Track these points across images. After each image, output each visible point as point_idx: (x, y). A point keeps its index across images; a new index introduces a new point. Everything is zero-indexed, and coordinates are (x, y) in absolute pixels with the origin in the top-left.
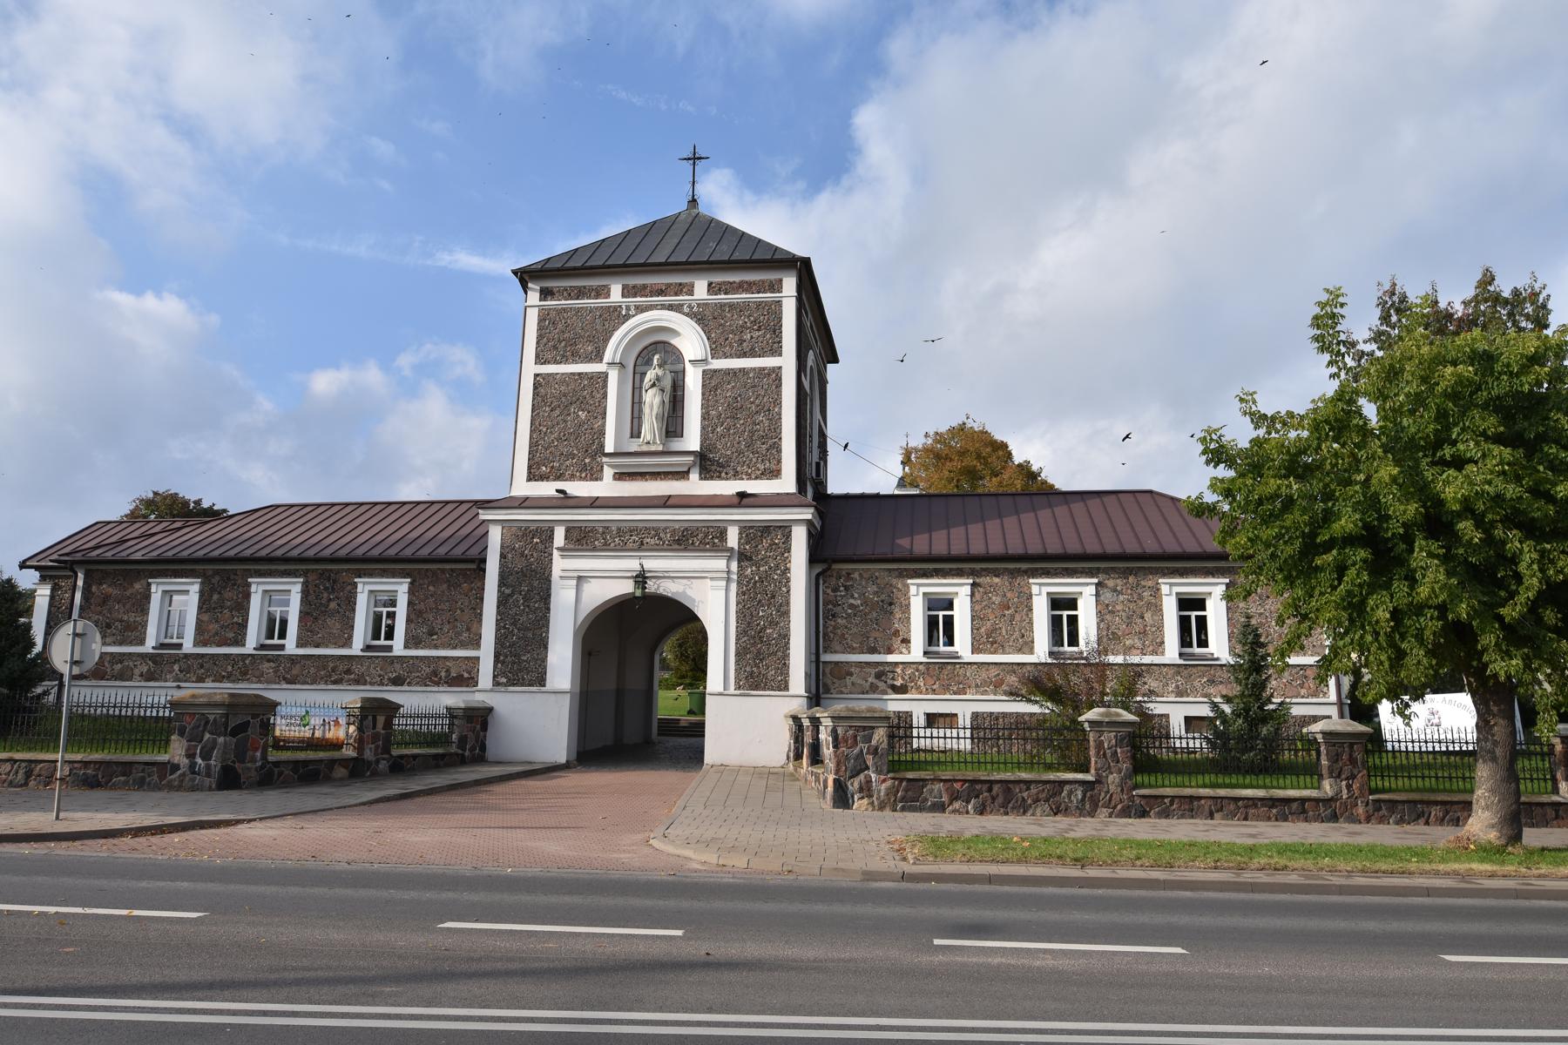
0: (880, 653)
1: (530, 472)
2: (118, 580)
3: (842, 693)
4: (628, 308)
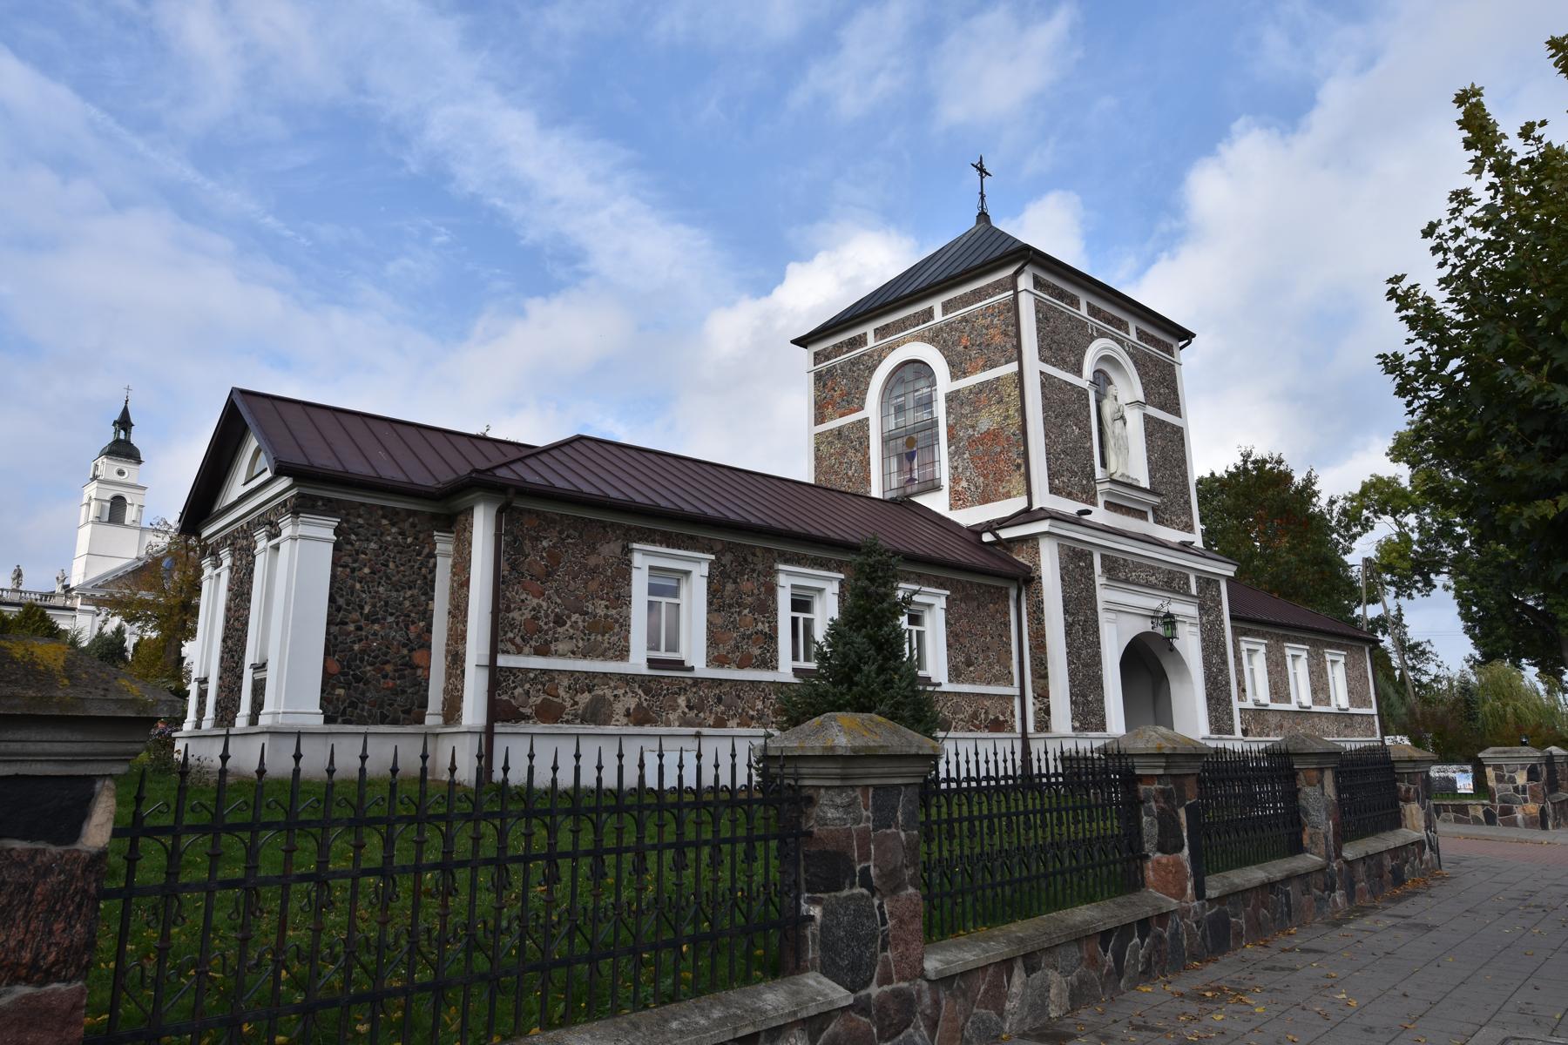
2: (568, 536)
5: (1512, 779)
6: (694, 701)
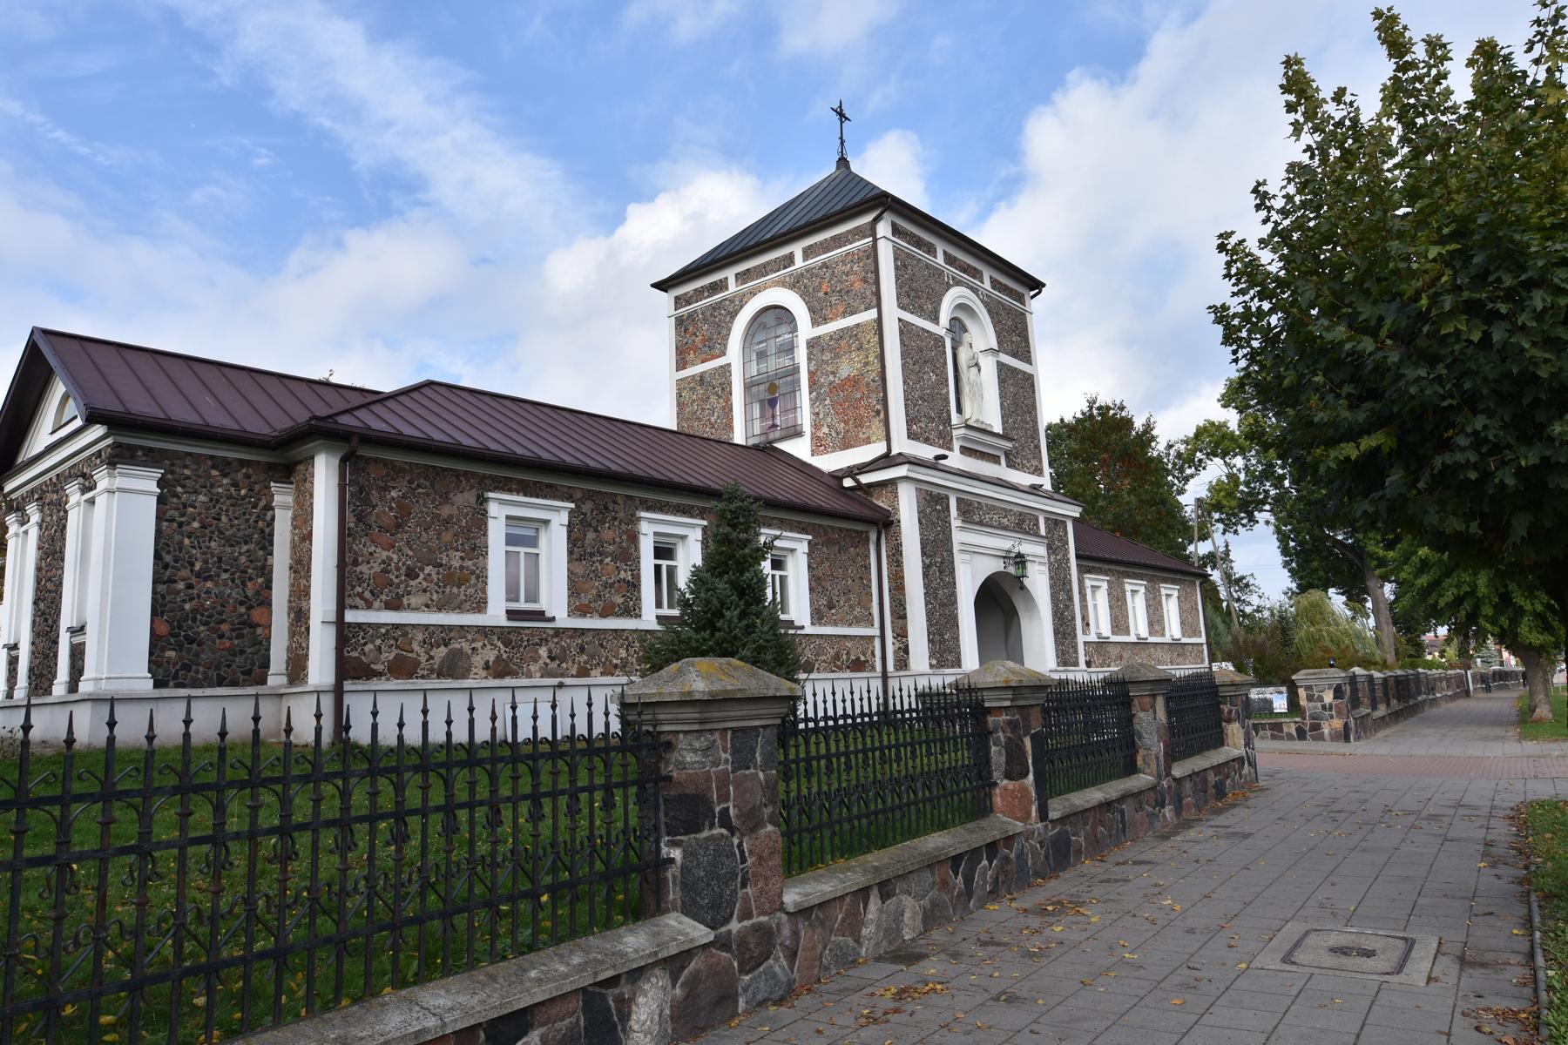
2: (419, 486)
5: (1321, 699)
6: (556, 651)
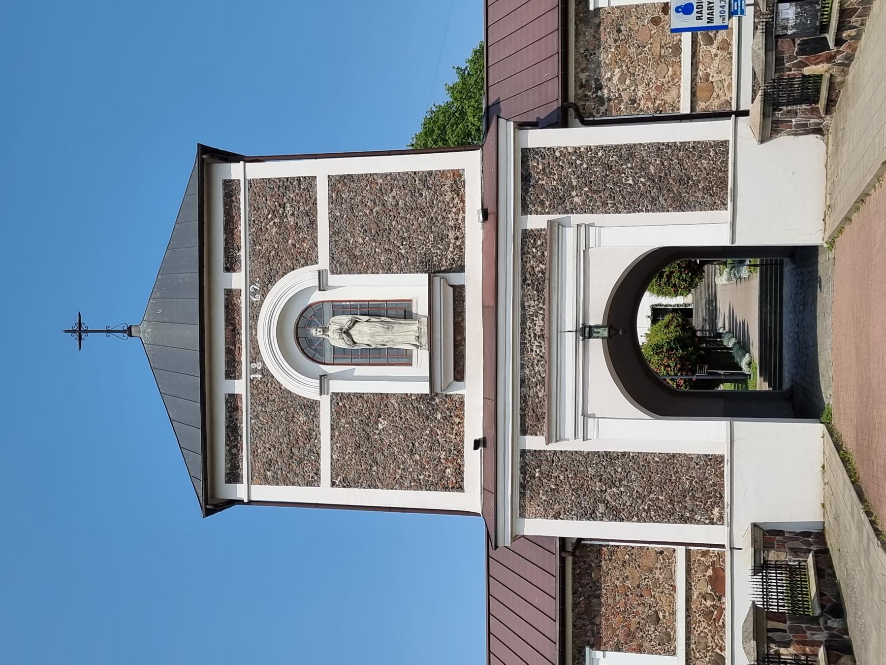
0: (680, 40)
1: (453, 488)
3: (730, 85)
4: (255, 371)
